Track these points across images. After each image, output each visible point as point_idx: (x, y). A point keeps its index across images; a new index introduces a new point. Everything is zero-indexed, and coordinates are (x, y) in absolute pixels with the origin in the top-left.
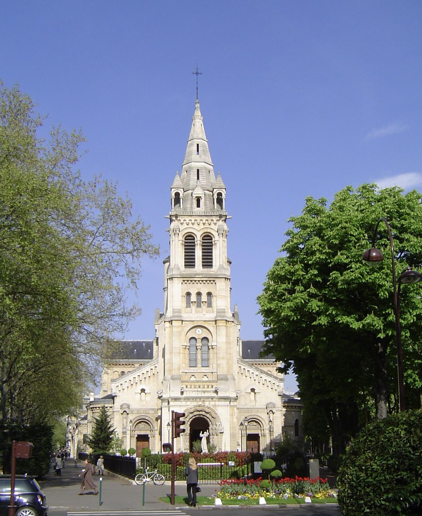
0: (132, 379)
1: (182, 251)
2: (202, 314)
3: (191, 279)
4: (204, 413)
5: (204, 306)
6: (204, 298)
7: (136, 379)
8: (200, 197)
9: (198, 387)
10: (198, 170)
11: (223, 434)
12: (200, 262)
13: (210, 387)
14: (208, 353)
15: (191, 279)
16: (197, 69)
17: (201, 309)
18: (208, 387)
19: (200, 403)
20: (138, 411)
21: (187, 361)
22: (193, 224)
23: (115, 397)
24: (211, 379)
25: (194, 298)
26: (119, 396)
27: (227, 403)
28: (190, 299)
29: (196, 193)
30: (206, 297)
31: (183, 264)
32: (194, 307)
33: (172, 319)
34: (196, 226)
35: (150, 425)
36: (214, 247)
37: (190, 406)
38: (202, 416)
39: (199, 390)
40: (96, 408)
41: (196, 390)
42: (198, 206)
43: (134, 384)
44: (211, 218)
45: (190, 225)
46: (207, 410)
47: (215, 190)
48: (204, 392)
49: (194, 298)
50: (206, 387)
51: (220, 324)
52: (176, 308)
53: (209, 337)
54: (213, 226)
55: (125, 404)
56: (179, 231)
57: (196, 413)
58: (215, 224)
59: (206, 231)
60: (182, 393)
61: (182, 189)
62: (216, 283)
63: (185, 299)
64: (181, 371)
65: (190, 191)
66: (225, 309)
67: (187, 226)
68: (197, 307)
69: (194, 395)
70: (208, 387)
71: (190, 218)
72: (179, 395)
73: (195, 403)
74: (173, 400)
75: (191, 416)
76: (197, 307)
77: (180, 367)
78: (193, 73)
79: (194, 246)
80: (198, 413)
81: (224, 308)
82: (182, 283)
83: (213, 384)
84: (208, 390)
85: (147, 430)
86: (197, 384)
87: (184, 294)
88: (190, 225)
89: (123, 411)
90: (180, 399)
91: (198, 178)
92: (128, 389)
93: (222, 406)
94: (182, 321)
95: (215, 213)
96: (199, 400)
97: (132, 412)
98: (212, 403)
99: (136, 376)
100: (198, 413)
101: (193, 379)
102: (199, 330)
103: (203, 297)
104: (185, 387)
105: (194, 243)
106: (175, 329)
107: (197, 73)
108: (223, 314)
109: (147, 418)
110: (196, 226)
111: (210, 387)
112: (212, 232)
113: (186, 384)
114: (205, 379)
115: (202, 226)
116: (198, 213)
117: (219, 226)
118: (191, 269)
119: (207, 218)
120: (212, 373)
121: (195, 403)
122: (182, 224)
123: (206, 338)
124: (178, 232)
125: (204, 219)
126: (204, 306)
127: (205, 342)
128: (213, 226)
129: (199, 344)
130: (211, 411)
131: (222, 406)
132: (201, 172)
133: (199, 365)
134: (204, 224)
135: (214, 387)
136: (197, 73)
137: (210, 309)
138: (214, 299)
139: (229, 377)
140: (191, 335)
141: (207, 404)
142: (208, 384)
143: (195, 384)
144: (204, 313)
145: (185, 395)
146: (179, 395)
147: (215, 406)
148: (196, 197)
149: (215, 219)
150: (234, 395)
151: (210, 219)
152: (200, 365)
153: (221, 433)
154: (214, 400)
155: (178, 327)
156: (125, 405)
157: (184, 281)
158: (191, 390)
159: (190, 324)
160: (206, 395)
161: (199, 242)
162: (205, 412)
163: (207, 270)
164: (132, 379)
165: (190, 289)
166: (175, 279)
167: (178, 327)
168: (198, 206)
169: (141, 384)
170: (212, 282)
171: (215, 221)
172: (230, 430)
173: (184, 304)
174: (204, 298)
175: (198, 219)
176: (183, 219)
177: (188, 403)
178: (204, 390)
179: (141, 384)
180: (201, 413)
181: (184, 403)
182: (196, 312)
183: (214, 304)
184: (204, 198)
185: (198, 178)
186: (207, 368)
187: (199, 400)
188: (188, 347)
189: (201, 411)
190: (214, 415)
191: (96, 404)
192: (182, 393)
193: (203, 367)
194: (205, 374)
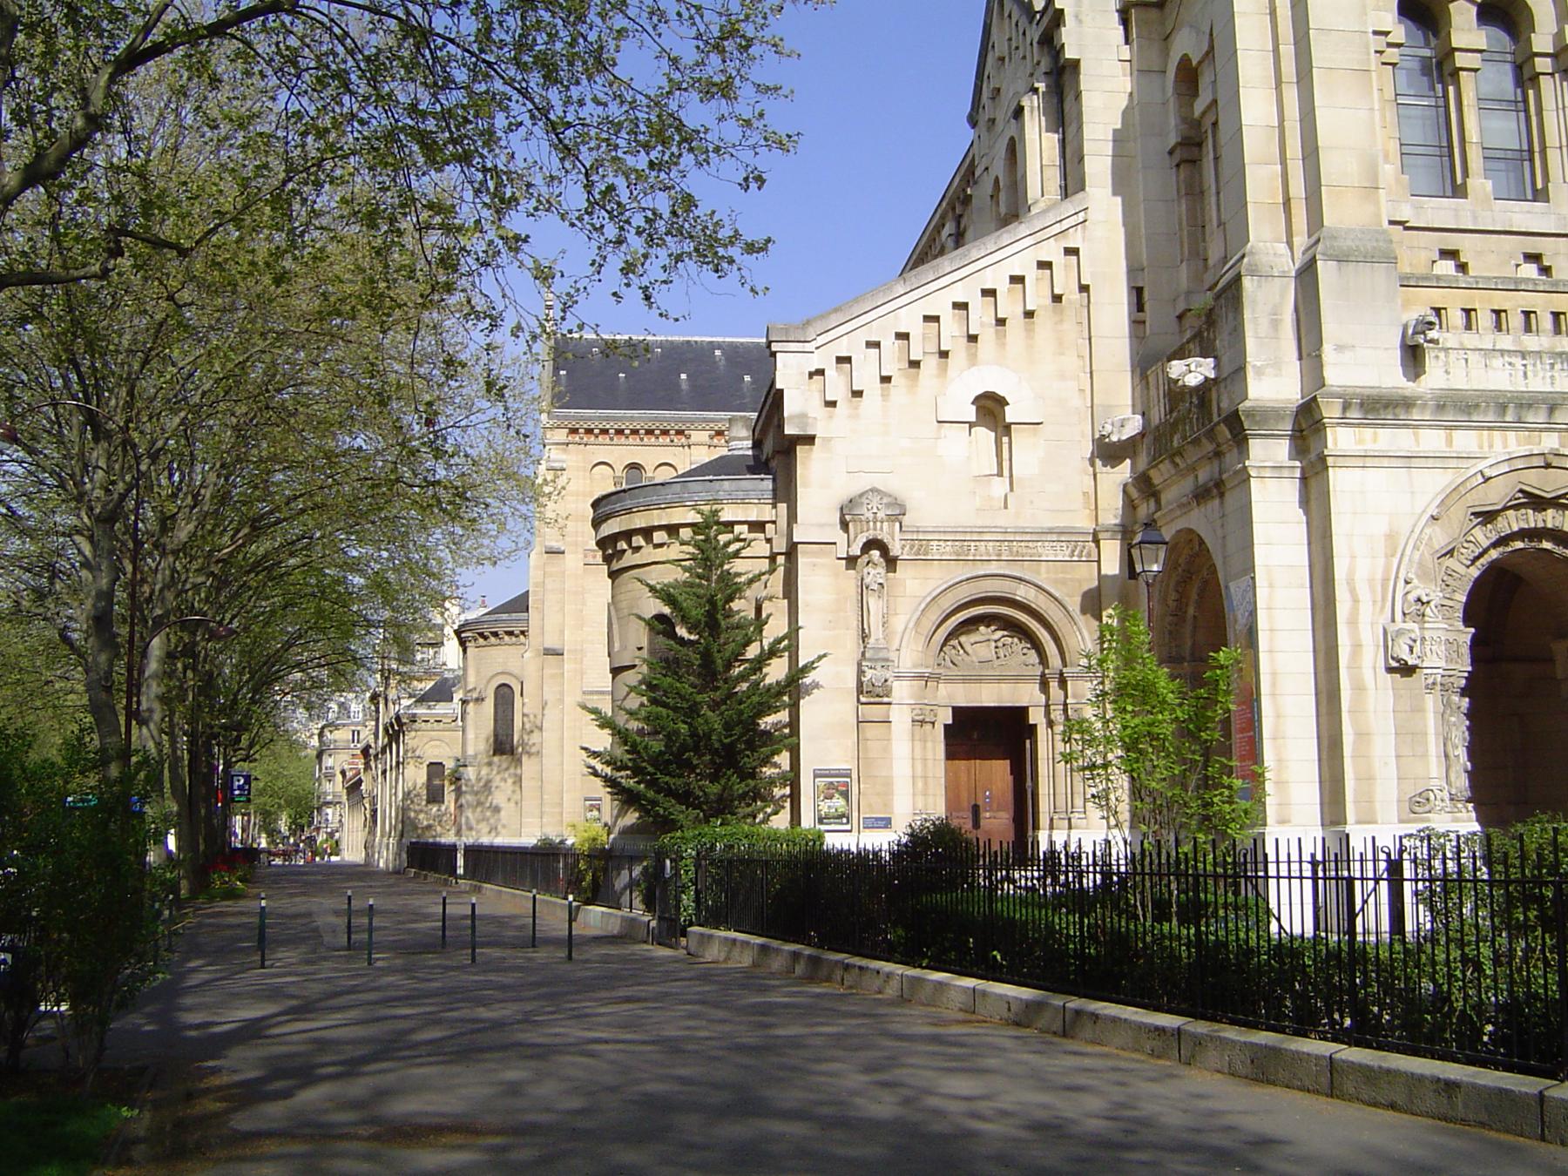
0: (916, 328)
20: (963, 542)
23: (801, 450)
26: (827, 440)
35: (1037, 646)
37: (1481, 465)
38: (1547, 545)
39: (1531, 342)
40: (647, 532)
41: (1505, 342)
43: (930, 364)
55: (873, 490)
57: (1513, 522)
60: (1413, 356)
72: (1388, 375)
73: (1512, 444)
74: (1354, 414)
80: (1532, 519)
85: (1018, 679)
89: (862, 540)
90: (1407, 403)
92: (885, 396)
96: (1542, 417)
97: (922, 556)
99: (940, 304)
100: (1532, 519)
109: (1022, 593)
145: (1436, 377)
146: (1388, 375)
156: (875, 501)
158: (1470, 339)
164: (910, 320)
169: (973, 360)
177: (1466, 441)
179: (973, 360)
181: (1432, 440)
187: (1537, 417)
191: (648, 507)
192: (1413, 356)
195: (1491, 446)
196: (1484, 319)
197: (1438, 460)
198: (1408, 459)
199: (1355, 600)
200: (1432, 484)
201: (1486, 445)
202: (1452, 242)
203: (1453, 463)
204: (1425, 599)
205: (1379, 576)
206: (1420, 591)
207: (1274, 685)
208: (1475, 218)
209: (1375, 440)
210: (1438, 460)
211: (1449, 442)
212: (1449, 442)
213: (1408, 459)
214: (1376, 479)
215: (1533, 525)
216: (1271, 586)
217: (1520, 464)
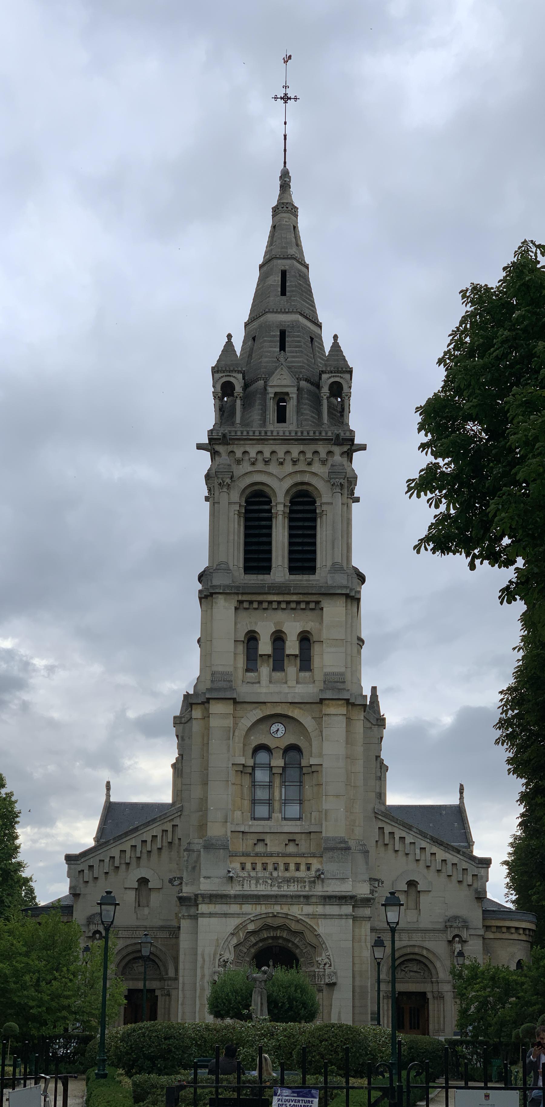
1: (239, 531)
2: (286, 685)
3: (260, 598)
4: (285, 935)
5: (292, 670)
6: (292, 647)
7: (128, 855)
8: (287, 394)
9: (270, 867)
10: (283, 334)
11: (336, 988)
12: (283, 557)
13: (303, 867)
14: (301, 784)
15: (260, 598)
16: (286, 87)
17: (283, 674)
18: (298, 869)
19: (277, 909)
21: (247, 803)
22: (267, 462)
24: (303, 848)
25: (265, 647)
27: (348, 909)
28: (256, 649)
29: (275, 383)
30: (297, 644)
31: (241, 564)
32: (265, 670)
33: (208, 696)
34: (273, 468)
36: (319, 520)
42: (282, 418)
44: (313, 447)
45: (260, 466)
46: (294, 926)
47: (324, 376)
48: (288, 881)
49: (265, 647)
50: (292, 867)
51: (331, 710)
52: (220, 669)
53: (302, 743)
54: (317, 467)
56: (232, 478)
57: (265, 935)
58: (324, 462)
59: (298, 479)
61: (240, 376)
62: (322, 609)
63: (241, 649)
64: (230, 827)
65: (262, 382)
66: (342, 674)
67: (250, 469)
68: (274, 669)
69: (262, 889)
70: (298, 869)
71: (259, 448)
73: (262, 909)
75: (254, 941)
76: (274, 669)
77: (227, 819)
78: (276, 98)
79: (270, 519)
81: (343, 670)
82: (236, 609)
83: (310, 860)
84: (298, 874)
86: (270, 861)
87: (241, 637)
88: (260, 466)
89: (92, 931)
91: (283, 348)
93: (331, 916)
94: (235, 702)
95: (323, 434)
98: (308, 909)
101: (260, 848)
102: (278, 728)
103: (288, 644)
104: (238, 866)
105: (269, 511)
106: (214, 722)
107: (286, 98)
108: (340, 686)
110: (273, 468)
111: (303, 867)
112: (314, 481)
113: (243, 859)
114: (291, 849)
115: (289, 468)
116: (281, 434)
117: (332, 465)
118: (261, 577)
119: (301, 448)
120: (310, 833)
121: (262, 909)
122: (239, 462)
123: (293, 749)
124: (228, 481)
125: (295, 450)
126: (292, 670)
127: (292, 754)
128: (317, 467)
129: (278, 762)
130: (303, 928)
131: (331, 916)
132: (289, 336)
133: (277, 815)
134: (295, 462)
135: (313, 868)
136: (286, 98)
137: (307, 674)
138: (316, 649)
139: (352, 844)
140: (255, 740)
141: (295, 910)
142: (298, 860)
143: (265, 860)
144: (292, 683)
147: (314, 916)
148: (276, 394)
149: (322, 449)
150: (363, 890)
151: (309, 449)
152: (280, 816)
153: (327, 984)
154: (314, 900)
155: (225, 716)
157: (240, 602)
158: (253, 874)
159: (254, 712)
160: (293, 889)
161: (280, 508)
162: (289, 930)
163: (302, 579)
165: (256, 623)
166: (220, 596)
167: (225, 716)
168: (282, 418)
170: (312, 605)
171: (323, 455)
172: (354, 977)
173: (241, 662)
174: (292, 647)
175: (281, 450)
176: (242, 450)
177: (247, 908)
178: (287, 874)
180: (278, 933)
181: (234, 908)
182: (270, 682)
183: (316, 662)
184: (295, 396)
185: (283, 348)
186: (298, 823)
188: (250, 770)
189: (278, 928)
190: (314, 941)
193: (285, 819)
194: (291, 837)
195: (256, 910)
196: (259, 867)
197: (238, 915)
198: (225, 915)
199: (204, 961)
200: (233, 923)
201: (254, 909)
202: (261, 837)
203: (241, 916)
204: (226, 960)
205: (212, 953)
206: (225, 958)
207: (183, 987)
208: (270, 828)
209: (215, 907)
210: (238, 915)
211: (241, 908)
212: (241, 908)
213: (225, 915)
214: (213, 920)
215: (272, 935)
216: (185, 954)
217: (263, 916)
